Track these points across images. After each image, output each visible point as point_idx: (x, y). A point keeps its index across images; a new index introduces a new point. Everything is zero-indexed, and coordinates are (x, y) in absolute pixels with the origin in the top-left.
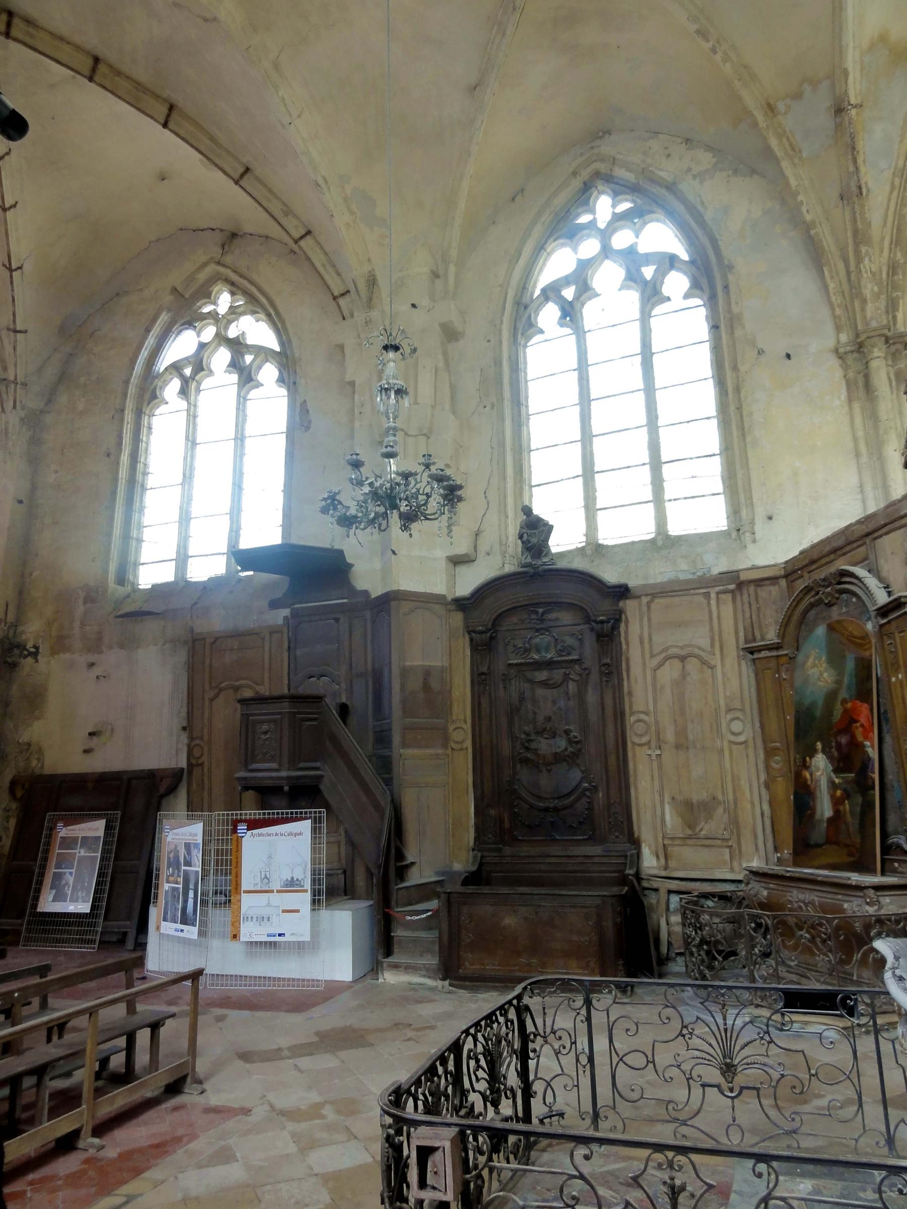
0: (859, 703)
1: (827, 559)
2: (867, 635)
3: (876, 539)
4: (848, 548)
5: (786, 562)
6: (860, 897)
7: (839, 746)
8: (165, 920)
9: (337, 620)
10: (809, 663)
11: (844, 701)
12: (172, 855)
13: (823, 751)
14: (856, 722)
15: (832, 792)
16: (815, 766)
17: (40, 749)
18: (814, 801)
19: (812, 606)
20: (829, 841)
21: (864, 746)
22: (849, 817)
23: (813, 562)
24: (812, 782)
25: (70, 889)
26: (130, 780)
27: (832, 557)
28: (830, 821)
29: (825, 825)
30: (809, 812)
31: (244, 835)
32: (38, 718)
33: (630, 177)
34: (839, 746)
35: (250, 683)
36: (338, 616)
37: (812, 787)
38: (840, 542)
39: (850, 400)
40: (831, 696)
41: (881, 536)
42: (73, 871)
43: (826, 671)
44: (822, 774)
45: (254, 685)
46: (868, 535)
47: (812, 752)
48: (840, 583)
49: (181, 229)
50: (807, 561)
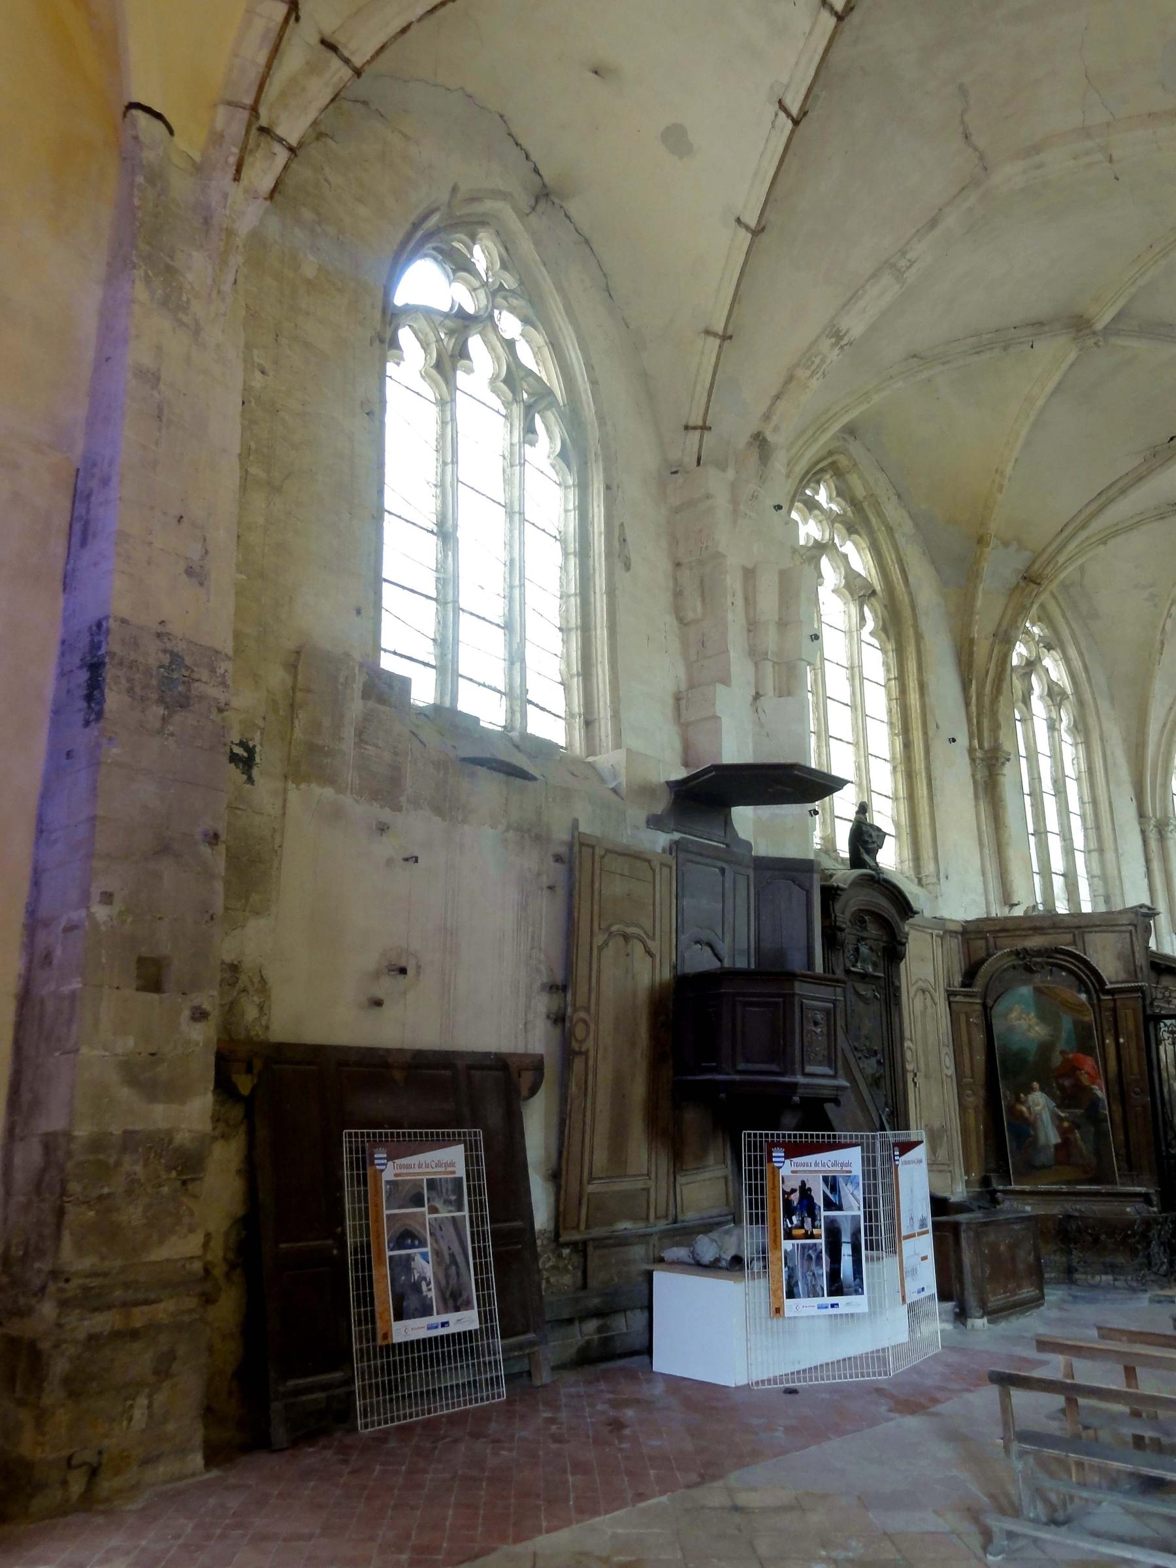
0: (1082, 1056)
1: (1023, 933)
4: (1051, 931)
5: (966, 922)
7: (1062, 1088)
8: (791, 1294)
9: (723, 871)
11: (1063, 1052)
12: (795, 1198)
13: (1042, 1090)
14: (1080, 1070)
15: (1057, 1123)
16: (1033, 1101)
17: (263, 981)
18: (1036, 1132)
19: (1014, 967)
21: (1092, 1089)
22: (1080, 1143)
25: (432, 1286)
26: (470, 1067)
27: (1031, 932)
28: (1057, 1146)
30: (1031, 1139)
31: (781, 1165)
32: (257, 913)
33: (860, 492)
34: (1062, 1088)
35: (643, 934)
36: (725, 865)
37: (1032, 1118)
38: (1046, 924)
39: (976, 797)
40: (1045, 1049)
41: (1091, 932)
42: (428, 1249)
43: (1037, 1025)
45: (645, 937)
46: (1079, 927)
47: (1029, 1090)
48: (1048, 957)
49: (502, 116)
50: (997, 928)
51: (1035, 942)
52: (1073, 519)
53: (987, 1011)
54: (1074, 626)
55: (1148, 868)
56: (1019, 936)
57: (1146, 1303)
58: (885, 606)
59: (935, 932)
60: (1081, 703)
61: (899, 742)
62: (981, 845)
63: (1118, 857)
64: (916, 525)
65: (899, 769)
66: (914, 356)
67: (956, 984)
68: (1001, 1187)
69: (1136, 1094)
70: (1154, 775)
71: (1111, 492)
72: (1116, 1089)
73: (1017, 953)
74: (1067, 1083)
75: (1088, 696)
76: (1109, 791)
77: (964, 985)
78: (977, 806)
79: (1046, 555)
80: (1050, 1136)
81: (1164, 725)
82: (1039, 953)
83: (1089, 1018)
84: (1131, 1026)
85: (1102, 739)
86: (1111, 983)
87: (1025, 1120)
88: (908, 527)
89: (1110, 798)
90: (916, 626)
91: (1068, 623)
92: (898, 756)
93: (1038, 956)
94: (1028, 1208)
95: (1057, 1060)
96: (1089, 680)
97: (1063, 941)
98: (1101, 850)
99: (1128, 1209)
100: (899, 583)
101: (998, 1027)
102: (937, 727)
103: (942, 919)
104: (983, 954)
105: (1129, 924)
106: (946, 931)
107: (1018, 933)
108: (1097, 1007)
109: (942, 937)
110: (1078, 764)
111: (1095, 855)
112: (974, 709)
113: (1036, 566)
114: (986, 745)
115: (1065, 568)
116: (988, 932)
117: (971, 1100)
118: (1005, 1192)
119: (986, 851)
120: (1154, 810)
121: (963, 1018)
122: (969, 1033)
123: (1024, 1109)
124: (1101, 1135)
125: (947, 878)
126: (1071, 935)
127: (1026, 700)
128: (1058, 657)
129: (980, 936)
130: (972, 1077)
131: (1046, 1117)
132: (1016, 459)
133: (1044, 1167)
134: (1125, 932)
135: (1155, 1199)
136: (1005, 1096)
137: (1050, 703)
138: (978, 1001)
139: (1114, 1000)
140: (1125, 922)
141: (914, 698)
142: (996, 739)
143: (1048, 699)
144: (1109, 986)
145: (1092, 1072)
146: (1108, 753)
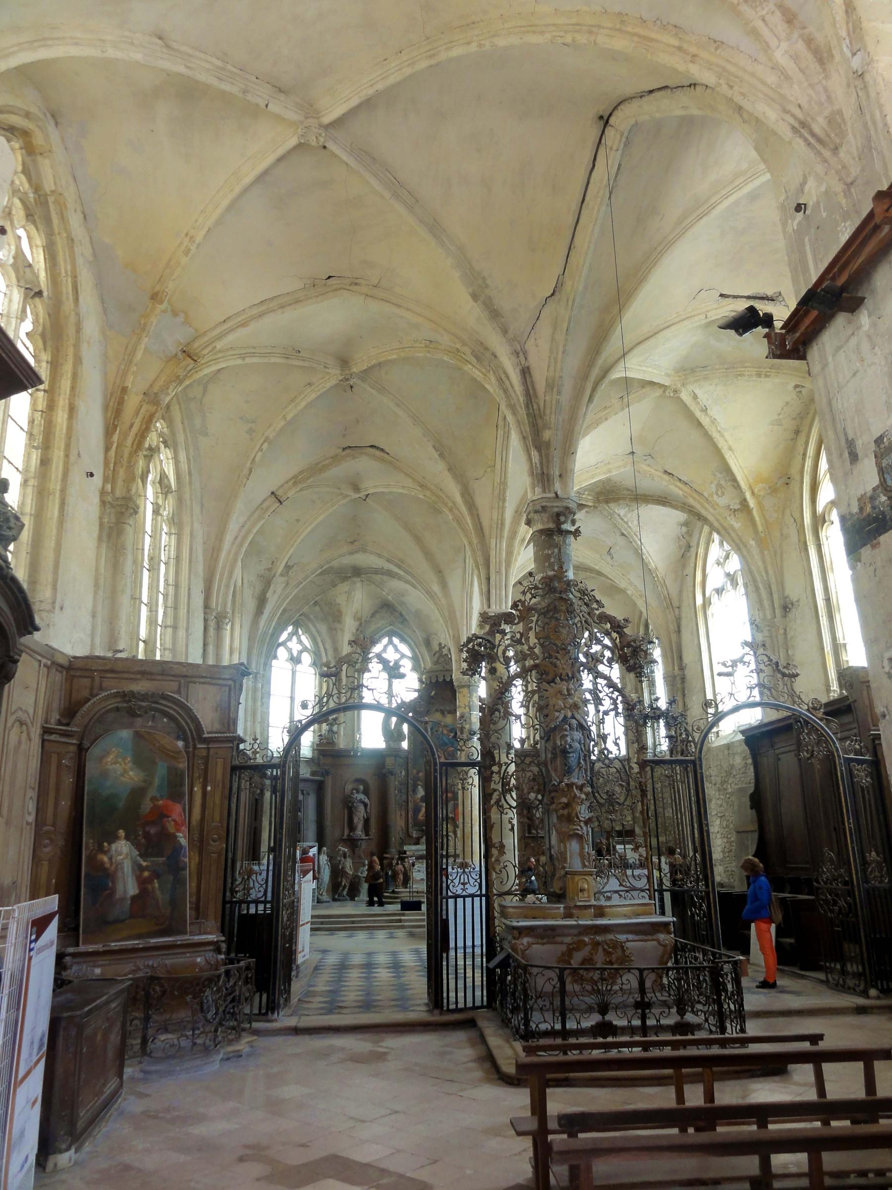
0: (170, 803)
1: (132, 676)
2: (180, 751)
3: (191, 682)
4: (158, 677)
5: (75, 657)
6: (211, 950)
7: (147, 835)
10: (109, 759)
11: (153, 799)
13: (127, 838)
14: (168, 817)
15: (138, 873)
16: (116, 851)
18: (113, 882)
19: (117, 709)
20: (132, 916)
21: (176, 837)
22: (158, 892)
23: (112, 671)
24: (111, 864)
27: (139, 676)
28: (134, 898)
29: (129, 902)
30: (108, 892)
33: (48, 185)
34: (147, 835)
39: (100, 539)
40: (138, 793)
41: (195, 683)
43: (132, 769)
44: (126, 858)
46: (186, 676)
47: (113, 838)
50: (107, 668)
51: (141, 686)
52: (237, 314)
53: (82, 751)
54: (188, 434)
55: (204, 650)
56: (127, 679)
57: (217, 1066)
58: (49, 315)
59: (44, 661)
60: (180, 501)
61: (35, 456)
62: (96, 585)
63: (187, 636)
64: (94, 255)
65: (31, 482)
66: (160, 38)
67: (53, 721)
68: (71, 950)
69: (214, 841)
70: (222, 575)
71: (272, 304)
72: (196, 837)
73: (123, 695)
74: (153, 830)
75: (187, 496)
76: (189, 578)
77: (59, 723)
78: (98, 547)
79: (206, 339)
80: (128, 886)
81: (236, 538)
82: (144, 697)
83: (183, 765)
84: (219, 775)
85: (191, 535)
86: (208, 733)
87: (106, 870)
88: (88, 251)
89: (189, 585)
90: (77, 346)
91: (184, 430)
92: (33, 469)
93: (143, 701)
94: (98, 971)
95: (147, 806)
96: (190, 483)
97: (169, 687)
98: (175, 627)
99: (199, 960)
100: (68, 298)
101: (91, 769)
102: (79, 455)
103: (51, 647)
104: (86, 693)
105: (229, 679)
106: (53, 663)
107: (126, 675)
108: (191, 756)
109: (48, 668)
110: (169, 551)
111: (169, 631)
112: (112, 453)
113: (196, 345)
114: (118, 493)
115: (210, 366)
116: (96, 671)
117: (47, 850)
118: (74, 955)
119: (101, 593)
120: (217, 605)
121: (54, 758)
122: (58, 775)
123: (105, 859)
124: (179, 882)
125: (62, 608)
126: (177, 683)
127: (144, 478)
128: (170, 456)
129: (86, 674)
130: (54, 825)
131: (127, 867)
132: (209, 229)
133: (117, 921)
134: (226, 685)
135: (224, 946)
136: (87, 844)
137: (159, 490)
138: (75, 742)
139: (208, 749)
140: (227, 677)
141: (61, 417)
142: (129, 490)
143: (158, 485)
144: (206, 735)
145: (177, 819)
146: (194, 548)
